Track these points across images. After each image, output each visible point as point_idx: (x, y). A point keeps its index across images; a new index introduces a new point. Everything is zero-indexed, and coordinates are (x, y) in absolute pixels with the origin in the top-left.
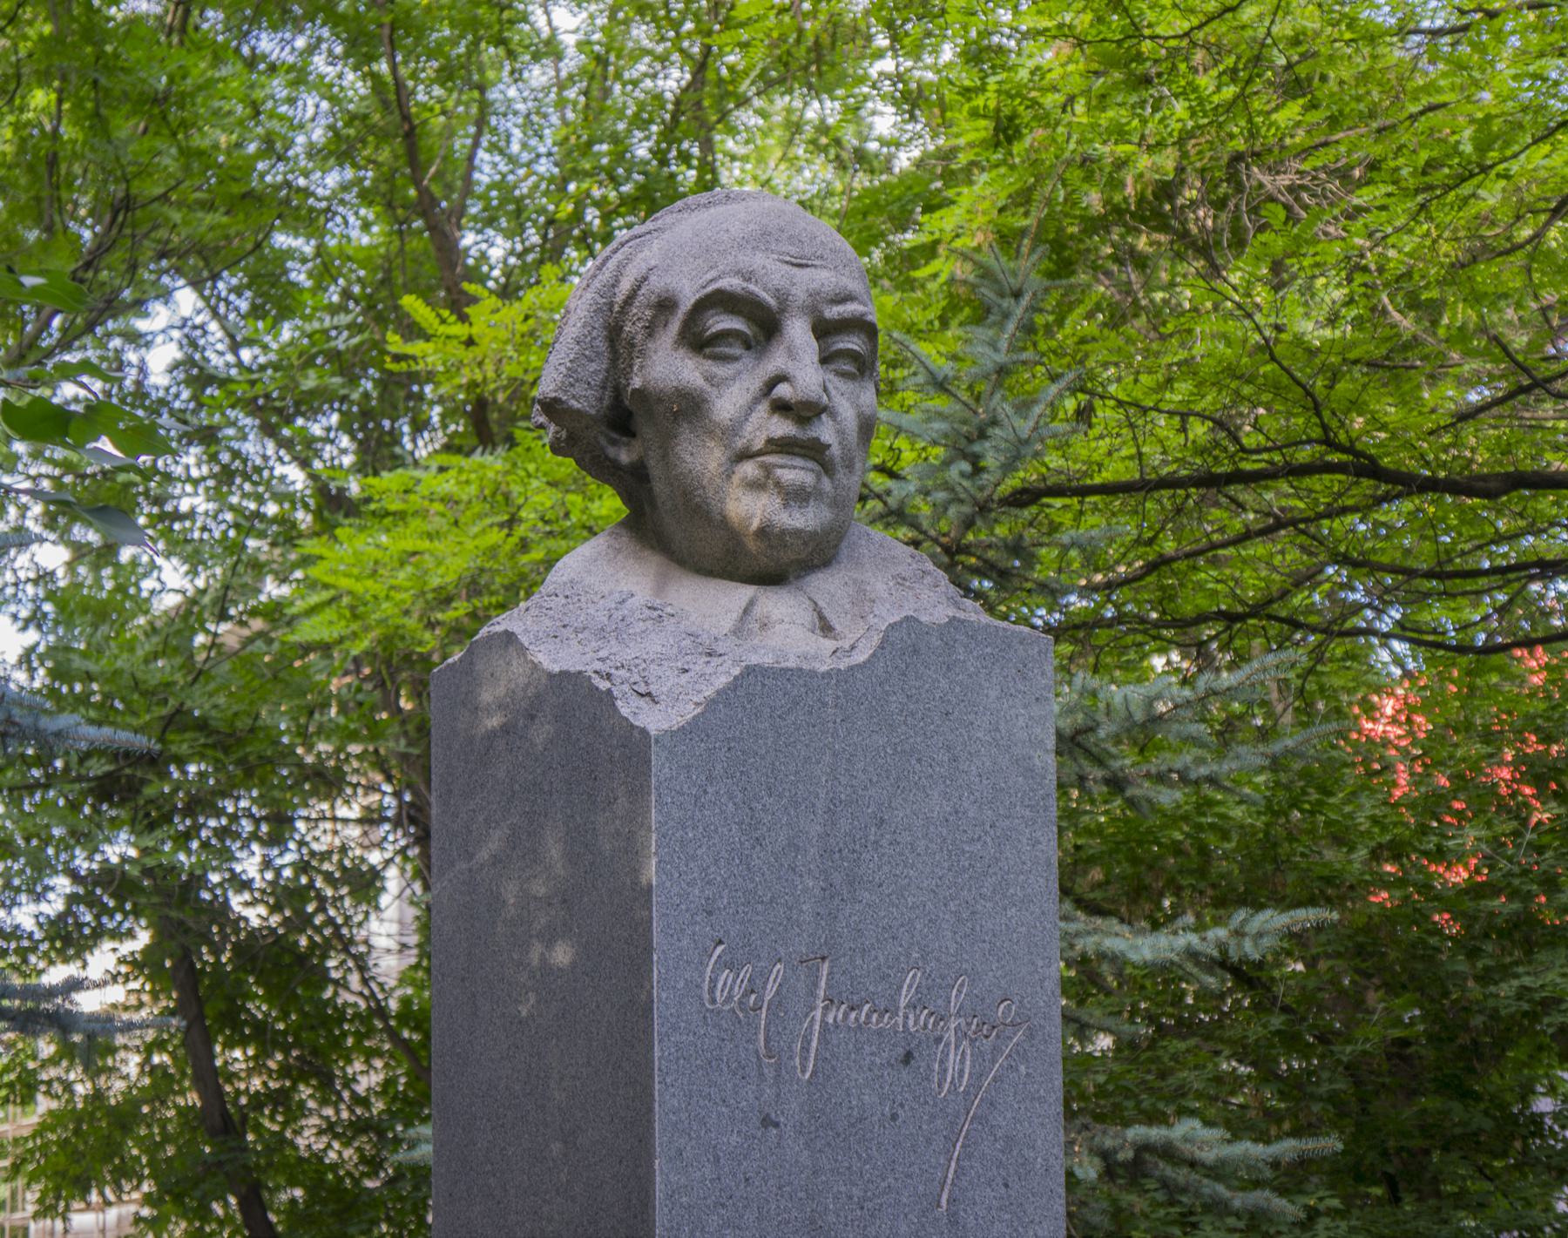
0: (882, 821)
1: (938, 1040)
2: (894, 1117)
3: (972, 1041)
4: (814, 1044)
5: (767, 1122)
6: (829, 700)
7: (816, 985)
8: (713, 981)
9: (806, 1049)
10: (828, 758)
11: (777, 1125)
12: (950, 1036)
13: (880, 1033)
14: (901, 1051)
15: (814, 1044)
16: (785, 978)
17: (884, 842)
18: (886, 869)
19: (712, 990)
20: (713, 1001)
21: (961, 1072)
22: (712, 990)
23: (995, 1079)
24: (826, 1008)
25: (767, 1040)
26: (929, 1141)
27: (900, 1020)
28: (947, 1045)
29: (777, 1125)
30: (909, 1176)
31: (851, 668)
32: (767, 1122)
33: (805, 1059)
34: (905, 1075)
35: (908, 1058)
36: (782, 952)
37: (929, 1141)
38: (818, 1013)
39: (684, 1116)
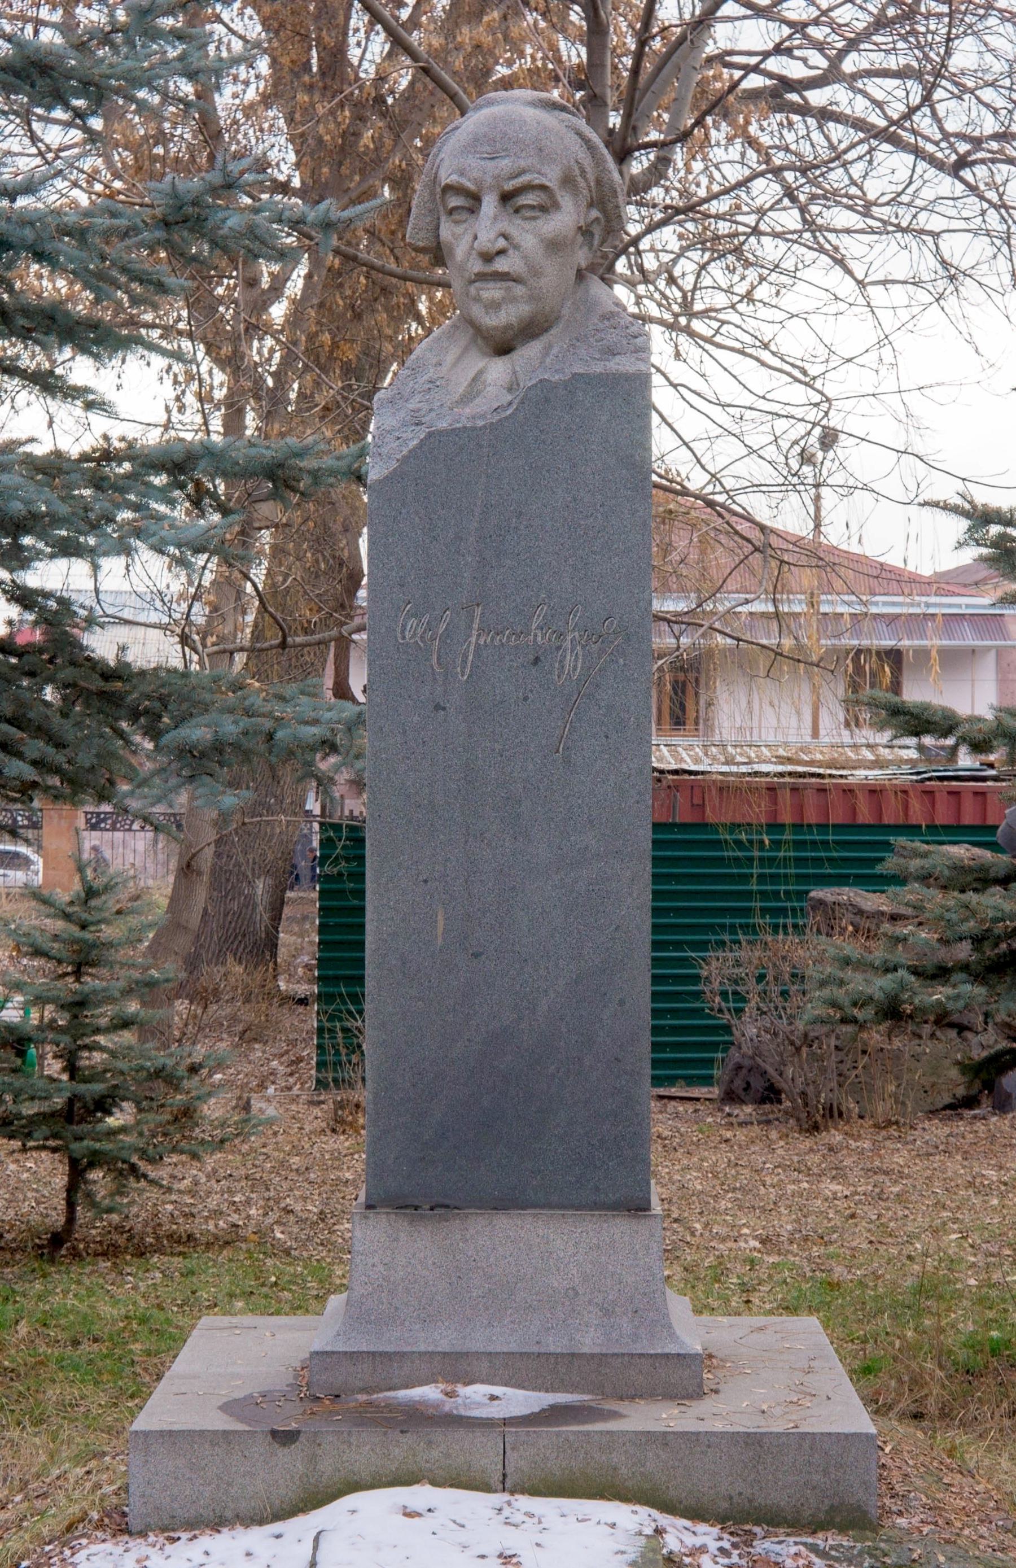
0: (521, 513)
1: (559, 648)
2: (526, 699)
3: (583, 647)
4: (470, 658)
5: (438, 707)
6: (484, 443)
7: (472, 622)
8: (404, 627)
9: (464, 661)
10: (483, 479)
11: (444, 709)
12: (568, 644)
13: (516, 647)
14: (531, 657)
15: (470, 658)
16: (451, 620)
17: (522, 527)
18: (523, 543)
19: (403, 632)
20: (404, 638)
21: (575, 668)
22: (403, 632)
23: (600, 670)
24: (479, 635)
25: (438, 659)
26: (550, 712)
27: (532, 638)
28: (565, 651)
29: (444, 709)
30: (536, 735)
31: (500, 420)
32: (438, 707)
33: (464, 668)
35: (536, 661)
36: (450, 603)
37: (550, 712)
38: (473, 639)
39: (384, 707)
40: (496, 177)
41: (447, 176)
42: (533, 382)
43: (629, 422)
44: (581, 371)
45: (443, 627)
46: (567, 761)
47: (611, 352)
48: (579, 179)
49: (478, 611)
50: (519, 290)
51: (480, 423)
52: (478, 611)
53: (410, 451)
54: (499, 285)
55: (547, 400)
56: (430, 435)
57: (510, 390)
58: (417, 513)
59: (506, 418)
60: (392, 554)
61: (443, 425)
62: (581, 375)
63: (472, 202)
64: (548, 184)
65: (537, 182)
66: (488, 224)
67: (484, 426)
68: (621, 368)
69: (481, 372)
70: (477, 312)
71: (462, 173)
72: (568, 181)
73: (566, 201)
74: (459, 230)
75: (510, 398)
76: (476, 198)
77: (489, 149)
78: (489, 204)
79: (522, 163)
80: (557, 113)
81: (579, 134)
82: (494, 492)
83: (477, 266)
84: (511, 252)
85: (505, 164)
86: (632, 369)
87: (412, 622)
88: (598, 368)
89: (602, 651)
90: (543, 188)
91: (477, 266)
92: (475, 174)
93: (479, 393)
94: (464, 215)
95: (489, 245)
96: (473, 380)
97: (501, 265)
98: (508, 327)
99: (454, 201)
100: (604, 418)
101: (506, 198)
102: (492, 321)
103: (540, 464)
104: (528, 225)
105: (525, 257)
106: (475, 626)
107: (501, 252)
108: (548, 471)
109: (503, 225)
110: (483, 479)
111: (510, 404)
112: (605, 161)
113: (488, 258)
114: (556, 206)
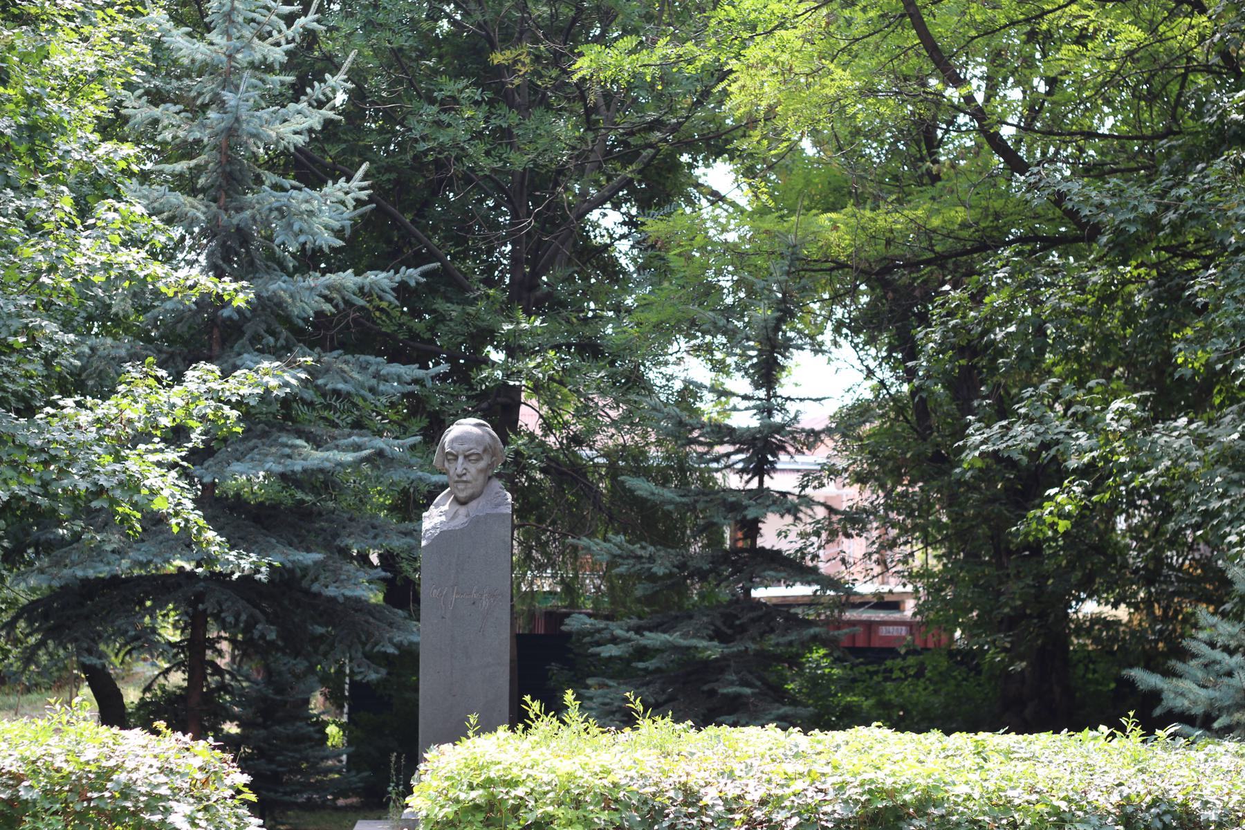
40: (464, 451)
47: (498, 505)
66: (460, 464)
72: (485, 450)
73: (485, 457)
76: (456, 458)
85: (466, 446)
88: (494, 511)
97: (464, 478)
101: (466, 457)
102: (462, 495)
113: (459, 476)
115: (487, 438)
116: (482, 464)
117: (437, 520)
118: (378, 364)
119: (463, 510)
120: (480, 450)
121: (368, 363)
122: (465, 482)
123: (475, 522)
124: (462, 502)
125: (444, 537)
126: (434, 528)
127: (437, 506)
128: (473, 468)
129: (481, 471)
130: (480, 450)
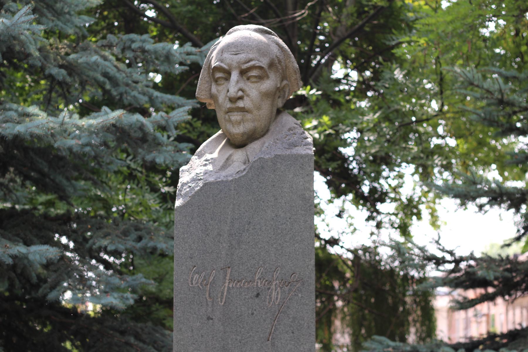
0: (250, 222)
1: (269, 289)
2: (253, 314)
3: (281, 288)
4: (225, 294)
5: (209, 318)
6: (232, 188)
7: (226, 276)
8: (192, 278)
9: (222, 295)
10: (231, 206)
11: (212, 319)
12: (273, 287)
13: (248, 288)
14: (255, 293)
15: (225, 294)
16: (216, 275)
17: (250, 229)
18: (251, 237)
19: (192, 281)
20: (192, 284)
21: (277, 298)
22: (192, 281)
23: (289, 299)
24: (229, 282)
25: (209, 294)
26: (265, 321)
27: (255, 284)
28: (272, 290)
29: (212, 319)
30: (257, 332)
31: (240, 177)
32: (209, 318)
33: (222, 299)
34: (257, 300)
35: (258, 295)
36: (215, 267)
37: (265, 321)
38: (227, 284)
39: (182, 318)
40: (239, 63)
41: (214, 64)
42: (256, 159)
43: (303, 178)
44: (279, 153)
45: (212, 278)
46: (273, 345)
48: (278, 65)
49: (229, 271)
50: (249, 116)
51: (230, 179)
52: (229, 271)
53: (195, 193)
54: (239, 113)
55: (263, 168)
56: (205, 185)
57: (245, 163)
58: (199, 223)
59: (243, 176)
60: (187, 242)
61: (211, 179)
62: (280, 155)
63: (226, 75)
64: (263, 66)
65: (257, 65)
66: (233, 86)
67: (232, 181)
68: (299, 152)
69: (231, 156)
70: (229, 127)
71: (222, 61)
72: (271, 65)
74: (220, 88)
75: (244, 167)
76: (228, 73)
77: (234, 50)
78: (235, 76)
79: (251, 56)
80: (267, 35)
81: (278, 44)
82: (236, 212)
83: (229, 105)
84: (245, 98)
85: (242, 57)
86: (304, 152)
87: (196, 276)
88: (288, 152)
89: (290, 290)
90: (261, 68)
91: (229, 105)
92: (228, 61)
93: (230, 165)
94: (223, 82)
95: (235, 94)
96: (227, 159)
97: (241, 104)
98: (243, 134)
99: (218, 75)
100: (290, 176)
101: (243, 73)
102: (238, 130)
103: (259, 198)
104: (252, 85)
105: (252, 100)
106: (228, 278)
107: (241, 98)
108: (263, 202)
109: (241, 85)
110: (231, 206)
111: (244, 170)
112: (290, 57)
114: (268, 77)
115: (275, 50)
116: (268, 85)
117: (200, 170)
118: (144, 41)
119: (239, 155)
120: (264, 62)
121: (133, 41)
122: (243, 110)
123: (257, 168)
124: (236, 144)
125: (209, 190)
126: (193, 180)
127: (200, 156)
128: (254, 90)
129: (266, 95)
130: (264, 62)
